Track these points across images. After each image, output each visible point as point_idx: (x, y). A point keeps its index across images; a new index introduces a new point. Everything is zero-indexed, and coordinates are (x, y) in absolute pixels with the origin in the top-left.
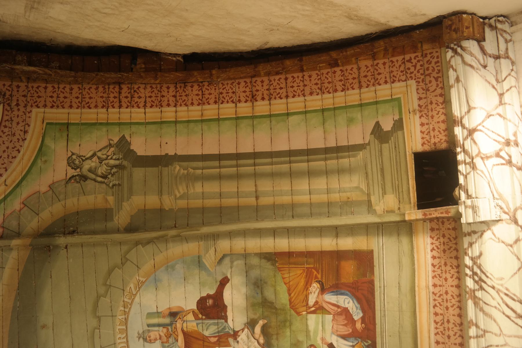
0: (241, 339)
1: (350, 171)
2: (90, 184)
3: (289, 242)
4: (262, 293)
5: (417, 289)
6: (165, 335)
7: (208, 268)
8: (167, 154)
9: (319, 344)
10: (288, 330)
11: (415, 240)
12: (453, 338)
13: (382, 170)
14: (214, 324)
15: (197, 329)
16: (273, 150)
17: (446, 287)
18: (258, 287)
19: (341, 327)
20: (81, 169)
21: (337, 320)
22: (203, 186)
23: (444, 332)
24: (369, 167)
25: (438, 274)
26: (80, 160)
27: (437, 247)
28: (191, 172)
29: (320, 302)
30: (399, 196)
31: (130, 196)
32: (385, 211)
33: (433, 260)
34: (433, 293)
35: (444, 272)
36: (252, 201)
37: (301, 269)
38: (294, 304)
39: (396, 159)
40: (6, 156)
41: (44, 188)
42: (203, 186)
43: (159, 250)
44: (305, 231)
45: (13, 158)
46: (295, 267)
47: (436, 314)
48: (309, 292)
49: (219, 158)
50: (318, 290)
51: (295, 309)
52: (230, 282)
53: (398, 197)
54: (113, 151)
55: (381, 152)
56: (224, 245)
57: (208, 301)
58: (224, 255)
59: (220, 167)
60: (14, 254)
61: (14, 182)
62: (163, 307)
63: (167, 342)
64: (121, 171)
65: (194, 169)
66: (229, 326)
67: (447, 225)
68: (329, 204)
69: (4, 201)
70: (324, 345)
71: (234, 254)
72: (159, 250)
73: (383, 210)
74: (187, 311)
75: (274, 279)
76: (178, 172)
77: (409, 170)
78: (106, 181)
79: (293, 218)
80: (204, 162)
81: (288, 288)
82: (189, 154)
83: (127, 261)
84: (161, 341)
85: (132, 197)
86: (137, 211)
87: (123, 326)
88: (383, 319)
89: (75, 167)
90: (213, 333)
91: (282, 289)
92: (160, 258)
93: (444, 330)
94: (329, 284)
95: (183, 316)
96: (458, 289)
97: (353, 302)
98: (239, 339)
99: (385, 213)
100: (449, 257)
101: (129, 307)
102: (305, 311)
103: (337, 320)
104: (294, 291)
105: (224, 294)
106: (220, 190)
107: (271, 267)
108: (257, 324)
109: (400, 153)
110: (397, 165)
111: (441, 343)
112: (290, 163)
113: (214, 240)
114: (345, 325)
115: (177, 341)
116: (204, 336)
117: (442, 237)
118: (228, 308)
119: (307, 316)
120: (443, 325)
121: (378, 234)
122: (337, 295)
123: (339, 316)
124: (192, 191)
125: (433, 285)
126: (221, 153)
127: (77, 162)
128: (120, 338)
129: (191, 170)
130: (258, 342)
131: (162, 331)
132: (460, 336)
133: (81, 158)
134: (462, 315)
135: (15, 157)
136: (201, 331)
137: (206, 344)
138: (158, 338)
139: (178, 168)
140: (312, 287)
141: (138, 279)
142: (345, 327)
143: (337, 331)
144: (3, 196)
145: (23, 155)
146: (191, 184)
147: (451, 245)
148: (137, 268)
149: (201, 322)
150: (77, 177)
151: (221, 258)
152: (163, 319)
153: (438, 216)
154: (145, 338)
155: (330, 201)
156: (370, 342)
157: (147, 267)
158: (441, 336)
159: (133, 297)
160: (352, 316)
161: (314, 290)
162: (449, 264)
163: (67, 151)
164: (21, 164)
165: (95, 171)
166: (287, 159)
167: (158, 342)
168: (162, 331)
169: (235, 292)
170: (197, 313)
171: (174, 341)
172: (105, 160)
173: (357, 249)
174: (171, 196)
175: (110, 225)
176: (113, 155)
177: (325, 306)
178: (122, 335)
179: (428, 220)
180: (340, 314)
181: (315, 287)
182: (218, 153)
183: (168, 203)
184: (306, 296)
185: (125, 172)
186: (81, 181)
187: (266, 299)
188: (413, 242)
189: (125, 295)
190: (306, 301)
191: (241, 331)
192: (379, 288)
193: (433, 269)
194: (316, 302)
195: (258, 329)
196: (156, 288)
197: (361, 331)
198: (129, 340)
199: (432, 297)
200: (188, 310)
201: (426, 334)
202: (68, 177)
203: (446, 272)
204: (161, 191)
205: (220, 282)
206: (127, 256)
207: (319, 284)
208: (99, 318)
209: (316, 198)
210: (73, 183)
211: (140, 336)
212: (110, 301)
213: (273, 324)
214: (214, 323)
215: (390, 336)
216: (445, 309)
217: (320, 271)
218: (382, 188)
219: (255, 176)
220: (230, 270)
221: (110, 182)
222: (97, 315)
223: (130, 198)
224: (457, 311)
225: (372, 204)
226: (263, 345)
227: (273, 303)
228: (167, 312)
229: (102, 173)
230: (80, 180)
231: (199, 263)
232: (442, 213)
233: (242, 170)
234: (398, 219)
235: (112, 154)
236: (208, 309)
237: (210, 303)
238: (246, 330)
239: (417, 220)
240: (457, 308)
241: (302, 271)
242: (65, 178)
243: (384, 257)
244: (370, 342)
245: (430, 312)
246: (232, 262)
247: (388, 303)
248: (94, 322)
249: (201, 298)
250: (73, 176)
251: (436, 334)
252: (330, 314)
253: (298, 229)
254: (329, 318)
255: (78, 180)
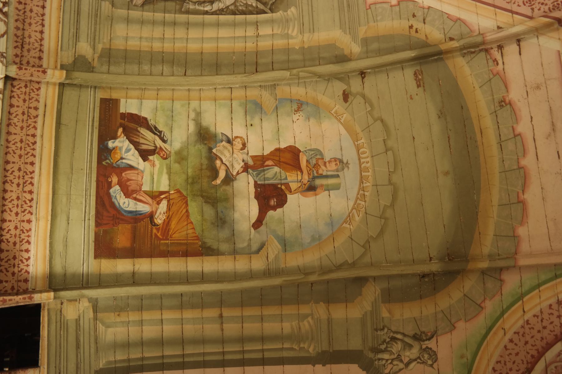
0: (240, 164)
1: (115, 346)
2: (410, 330)
3: (187, 267)
4: (217, 212)
5: (50, 218)
6: (320, 167)
7: (275, 239)
8: (324, 365)
9: (158, 160)
10: (190, 174)
11: (46, 270)
12: (16, 169)
13: (78, 347)
14: (268, 179)
15: (286, 173)
16: (202, 370)
17: (16, 220)
18: (221, 219)
19: (133, 178)
20: (421, 348)
21: (138, 185)
22: (282, 329)
23: (25, 174)
24: (93, 350)
25: (24, 233)
26: (422, 359)
27: (22, 262)
28: (296, 344)
29: (155, 204)
30: (61, 318)
31: (363, 317)
32: (78, 301)
33: (28, 248)
34: (32, 214)
35: (18, 236)
36: (227, 313)
37: (174, 238)
38: (182, 202)
39: (60, 360)
40: (507, 363)
41: (461, 325)
42: (282, 329)
43: (329, 258)
44: (169, 280)
45: (500, 362)
46: (181, 240)
47: (31, 192)
48: (166, 214)
49: (264, 360)
50: (156, 216)
51: (182, 196)
52: (251, 224)
53: (62, 317)
54: (385, 369)
55: (77, 368)
56: (258, 264)
57: (275, 203)
58: (259, 253)
59: (263, 351)
60: (486, 250)
61: (495, 333)
62: (322, 196)
63: (317, 160)
64: (375, 346)
65: (292, 349)
66: (253, 178)
67: (8, 286)
68: (141, 309)
69: (503, 310)
70: (153, 159)
71: (247, 254)
72: (329, 258)
73: (81, 301)
74: (298, 192)
75: (204, 227)
76: (311, 345)
77: (46, 347)
78: (392, 334)
79: (182, 294)
80: (281, 356)
81: (189, 218)
82: (299, 366)
83: (364, 245)
84: (324, 160)
85: (361, 316)
86: (355, 301)
87: (366, 176)
88: (88, 187)
89: (427, 350)
90: (268, 171)
91: (195, 217)
92: (328, 249)
93: (24, 176)
94: (144, 223)
95: (301, 187)
96: (3, 218)
97: (119, 204)
98: (242, 164)
99: (78, 299)
100: (10, 251)
101: (359, 196)
102: (171, 194)
103: (138, 185)
104: (183, 215)
105: (258, 211)
106: (262, 324)
107: (206, 240)
108: (223, 180)
109: (55, 367)
110: (60, 353)
111: (29, 164)
112: (183, 355)
113: (269, 269)
114: (129, 180)
115: (307, 161)
116: (279, 166)
117: (15, 273)
118: (254, 196)
119: (170, 189)
120: (24, 181)
121: (88, 275)
122: (136, 211)
123: (135, 189)
124: (293, 323)
125: (31, 221)
126: (262, 367)
127: (426, 356)
128: (367, 163)
129: (296, 347)
130: (222, 161)
131: (323, 171)
132: (7, 171)
133: (421, 360)
134: (3, 192)
135: (497, 362)
136: (283, 172)
137: (277, 158)
138: (327, 163)
139: (311, 350)
140: (163, 219)
141: (351, 226)
142: (129, 178)
143: (138, 174)
144: (505, 316)
145: (488, 365)
146: (296, 331)
147: (6, 264)
148: (353, 237)
149: (282, 181)
150: (424, 338)
151: (261, 249)
152: (322, 183)
153: (15, 297)
154: (342, 164)
155: (140, 312)
156: (104, 163)
157: (341, 240)
158: (27, 170)
159: (356, 206)
160: (121, 189)
161: (161, 216)
162: (11, 244)
163: (438, 369)
164: (489, 355)
165: (404, 346)
166: (186, 360)
167: (327, 159)
168: (323, 171)
169: (246, 213)
170: (287, 190)
171: (311, 160)
172: (394, 359)
173: (112, 260)
174: (317, 319)
175: (385, 285)
176: (386, 365)
177: (149, 200)
178: (365, 166)
179: (30, 291)
180: (134, 191)
181: (159, 219)
182: (265, 367)
183: (321, 310)
184: (169, 210)
185: (370, 345)
186: (419, 334)
187: (213, 206)
188: (49, 267)
189: (364, 208)
190: (170, 204)
191: (239, 172)
192: (90, 218)
193: (29, 239)
194: (158, 203)
195: (222, 174)
196: (331, 216)
197: (113, 174)
198: (358, 160)
199: (33, 210)
200: (296, 193)
201: (44, 172)
202: (435, 338)
203: (15, 236)
204: (329, 323)
205: (262, 224)
206: (363, 250)
207: (154, 223)
208: (390, 183)
209: (156, 315)
210: (428, 332)
211: (347, 165)
212: (380, 201)
213: (205, 181)
214: (268, 180)
215: (82, 169)
216: (20, 197)
217: (154, 237)
218: (80, 326)
219: (223, 340)
220: (252, 236)
221: (387, 333)
222: (392, 186)
223: (363, 315)
224: (7, 196)
225: (93, 309)
226: (216, 159)
227: (205, 202)
228: (318, 190)
229: (397, 343)
230: (421, 334)
231: (285, 244)
232: (10, 300)
233: (237, 348)
234: (63, 294)
235: (387, 365)
236: (275, 194)
237: (273, 201)
238: (234, 174)
239: (41, 292)
240: (7, 199)
241: (174, 236)
242: (438, 338)
243: (82, 251)
244: (104, 163)
245: (38, 194)
246: (249, 245)
247: (82, 203)
248: (396, 178)
249: (283, 207)
250: (429, 339)
251: (33, 172)
252: (145, 192)
253: (176, 282)
254: (146, 188)
255: (423, 335)
